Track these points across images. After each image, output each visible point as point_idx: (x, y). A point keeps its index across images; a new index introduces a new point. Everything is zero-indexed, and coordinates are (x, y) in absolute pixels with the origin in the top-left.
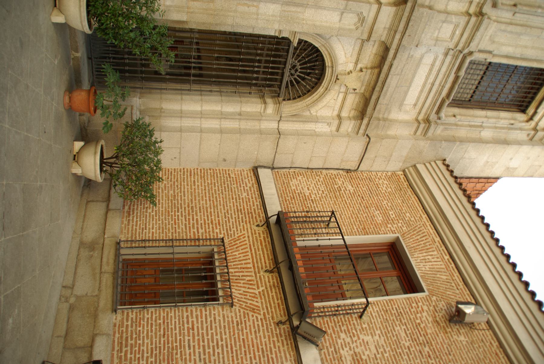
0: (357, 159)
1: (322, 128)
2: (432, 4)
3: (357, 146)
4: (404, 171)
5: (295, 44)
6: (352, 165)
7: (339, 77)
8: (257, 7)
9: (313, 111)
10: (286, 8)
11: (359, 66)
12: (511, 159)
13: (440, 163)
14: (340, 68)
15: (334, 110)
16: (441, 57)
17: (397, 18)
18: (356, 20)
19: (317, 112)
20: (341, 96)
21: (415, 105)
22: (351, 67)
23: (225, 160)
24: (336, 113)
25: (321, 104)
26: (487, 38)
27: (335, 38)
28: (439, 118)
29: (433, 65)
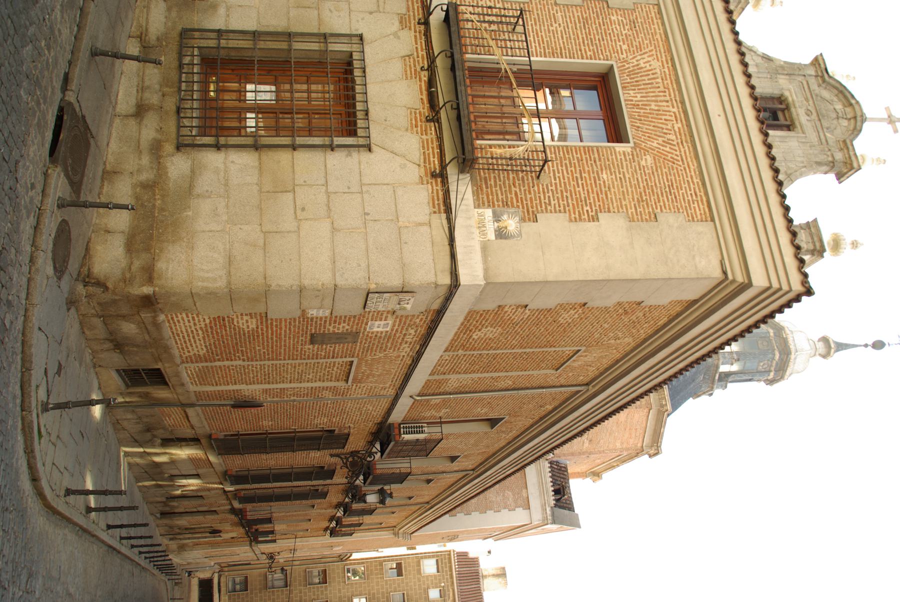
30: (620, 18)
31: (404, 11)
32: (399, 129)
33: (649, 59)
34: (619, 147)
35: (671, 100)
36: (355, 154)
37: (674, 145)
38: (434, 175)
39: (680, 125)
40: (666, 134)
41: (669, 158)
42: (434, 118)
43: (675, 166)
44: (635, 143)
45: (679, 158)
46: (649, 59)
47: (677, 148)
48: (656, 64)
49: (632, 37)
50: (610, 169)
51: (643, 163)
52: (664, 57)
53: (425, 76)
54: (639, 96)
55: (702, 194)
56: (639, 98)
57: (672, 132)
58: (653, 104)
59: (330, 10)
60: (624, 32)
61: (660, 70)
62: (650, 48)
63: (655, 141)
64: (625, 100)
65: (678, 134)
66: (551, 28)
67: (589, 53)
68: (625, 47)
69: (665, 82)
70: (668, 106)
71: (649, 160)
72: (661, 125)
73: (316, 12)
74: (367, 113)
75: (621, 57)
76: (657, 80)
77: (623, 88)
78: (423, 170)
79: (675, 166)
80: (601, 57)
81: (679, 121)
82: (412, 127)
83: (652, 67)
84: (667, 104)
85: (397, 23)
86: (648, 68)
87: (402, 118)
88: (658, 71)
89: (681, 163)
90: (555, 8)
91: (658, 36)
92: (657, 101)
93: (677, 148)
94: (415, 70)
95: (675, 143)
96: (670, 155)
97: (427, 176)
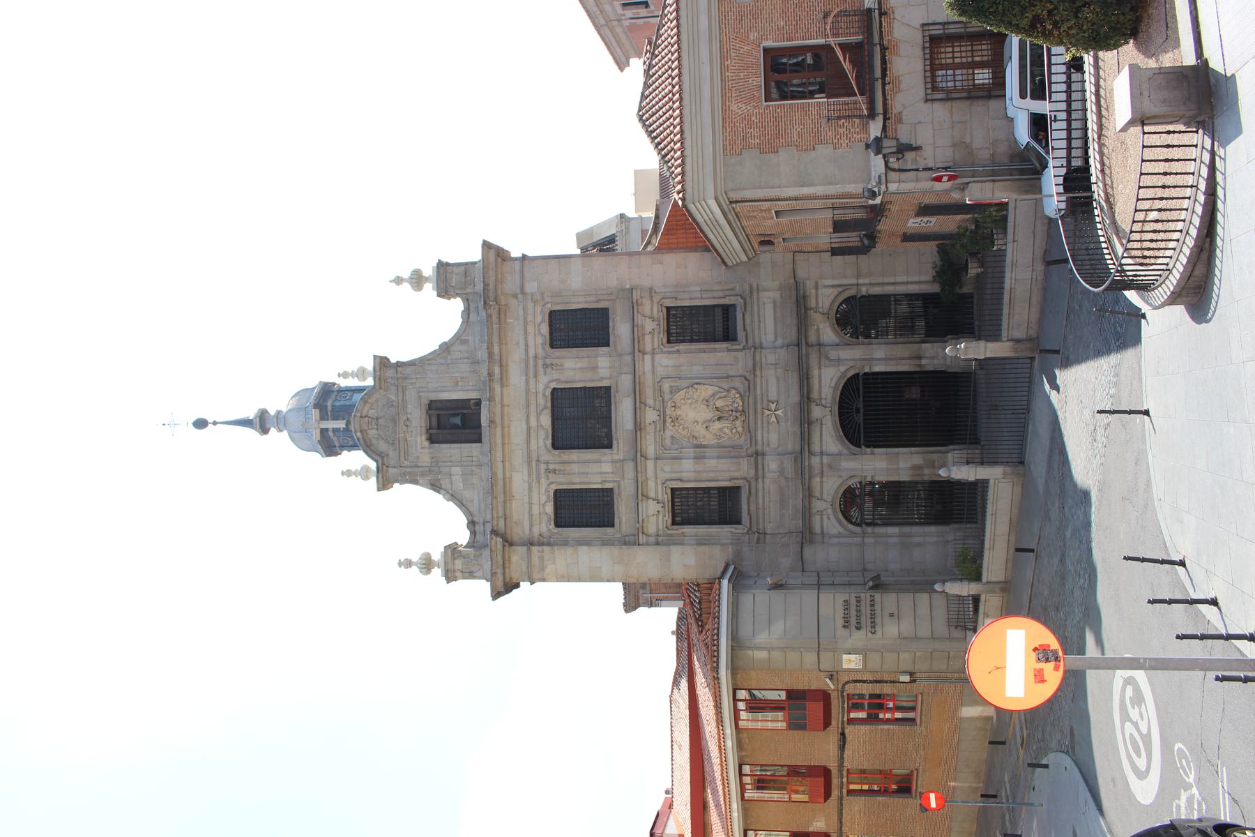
0: (798, 262)
1: (829, 282)
2: (786, 372)
3: (801, 273)
4: (756, 254)
5: (860, 337)
6: (799, 257)
7: (827, 320)
8: (886, 355)
9: (836, 293)
10: (871, 357)
11: (816, 327)
12: (664, 273)
13: (730, 264)
14: (827, 324)
15: (822, 294)
16: (763, 341)
17: (808, 364)
18: (830, 356)
19: (833, 292)
20: (820, 305)
21: (764, 304)
22: (821, 326)
23: (890, 255)
24: (820, 292)
25: (832, 297)
26: (740, 359)
27: (838, 343)
28: (742, 298)
29: (765, 334)
30: (753, 141)
31: (899, 125)
32: (905, 41)
33: (738, 111)
34: (769, 44)
35: (728, 82)
36: (931, 22)
37: (733, 49)
38: (885, 13)
39: (726, 63)
40: (737, 56)
41: (738, 39)
42: (884, 49)
43: (735, 35)
44: (759, 46)
45: (731, 40)
46: (738, 111)
47: (732, 47)
48: (734, 107)
49: (747, 126)
50: (778, 28)
51: (756, 34)
52: (727, 114)
53: (887, 79)
54: (750, 82)
55: (721, 17)
56: (750, 80)
57: (732, 58)
58: (742, 77)
59: (945, 122)
60: (752, 130)
61: (732, 102)
62: (736, 120)
63: (745, 50)
64: (761, 77)
65: (729, 57)
66: (802, 127)
67: (779, 110)
68: (754, 118)
69: (730, 94)
70: (732, 77)
71: (751, 37)
72: (739, 62)
73: (954, 119)
74: (924, 48)
75: (757, 111)
76: (735, 95)
77: (761, 86)
78: (891, 17)
79: (735, 35)
80: (771, 108)
81: (726, 66)
82: (897, 44)
83: (737, 105)
84: (732, 78)
85: (904, 117)
86: (740, 104)
87: (904, 49)
88: (733, 102)
89: (731, 37)
90: (798, 143)
91: (728, 130)
92: (739, 79)
93: (732, 47)
94: (893, 84)
95: (732, 51)
96: (737, 41)
97: (890, 14)
